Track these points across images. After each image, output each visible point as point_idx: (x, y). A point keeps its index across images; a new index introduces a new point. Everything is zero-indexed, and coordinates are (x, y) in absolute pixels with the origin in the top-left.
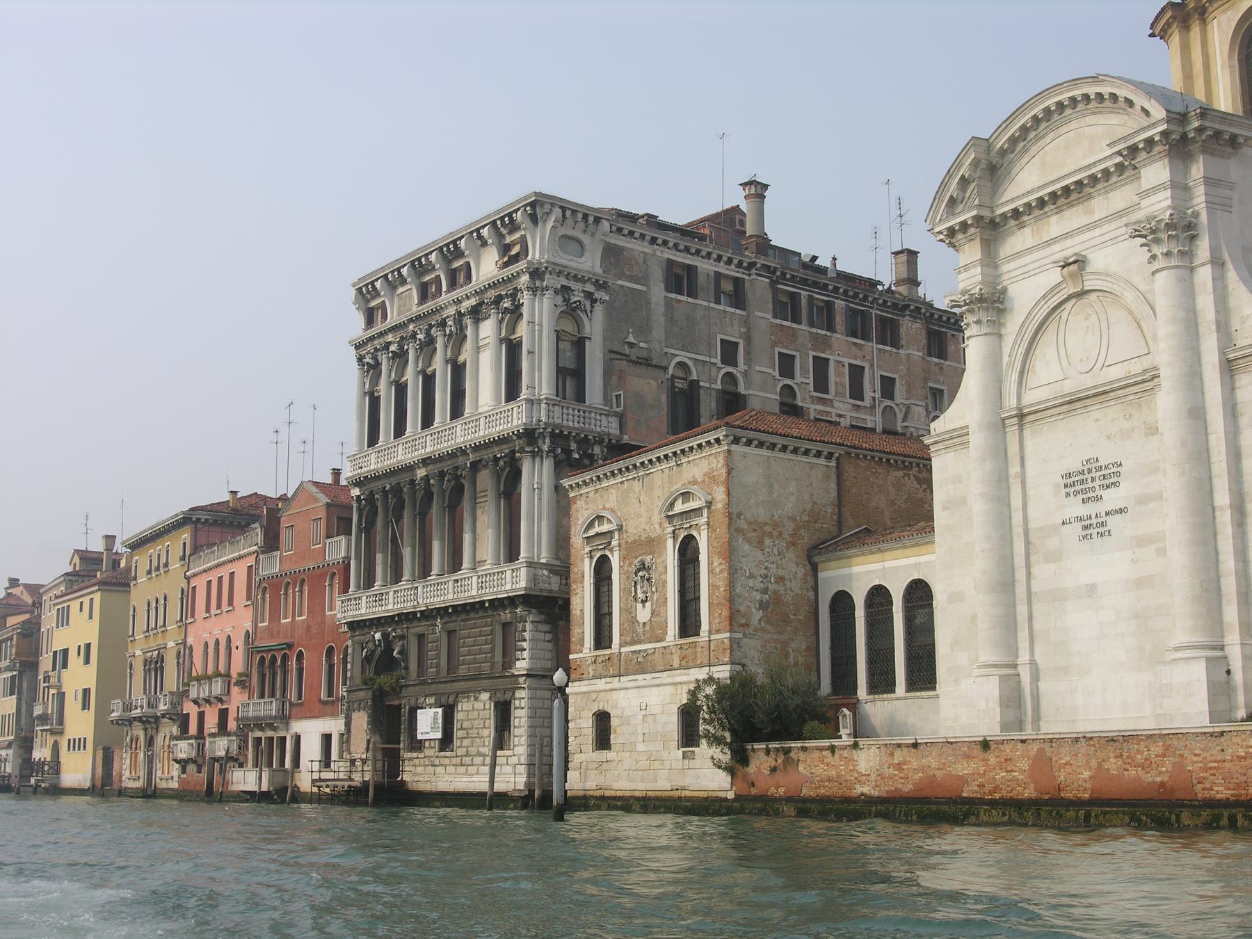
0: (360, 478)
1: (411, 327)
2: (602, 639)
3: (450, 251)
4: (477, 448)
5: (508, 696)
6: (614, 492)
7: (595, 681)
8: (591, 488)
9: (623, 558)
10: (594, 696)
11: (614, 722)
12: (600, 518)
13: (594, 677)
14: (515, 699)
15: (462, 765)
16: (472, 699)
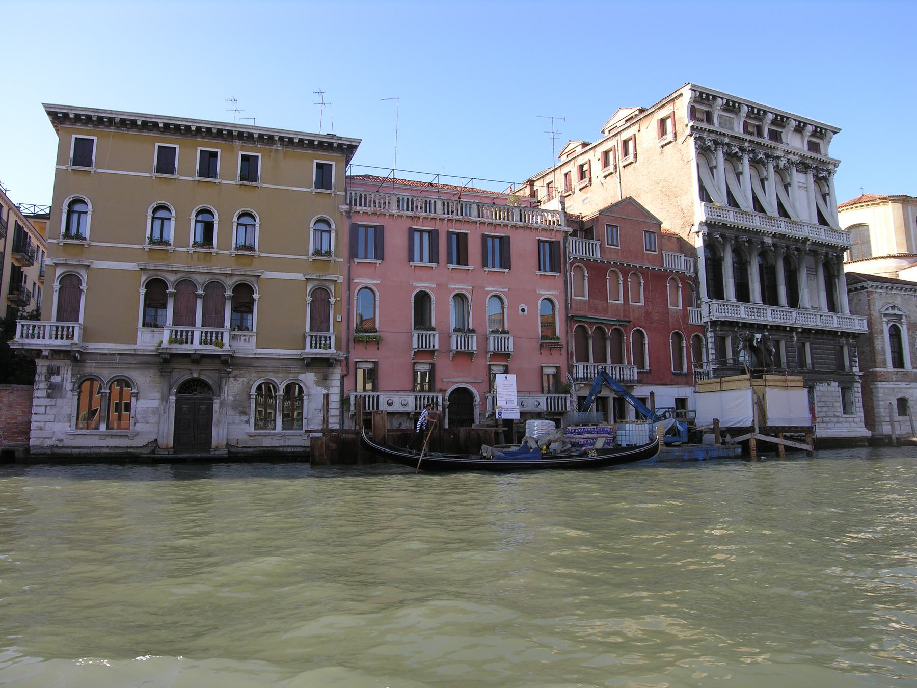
0: (719, 223)
1: (746, 144)
2: (899, 362)
3: (781, 120)
4: (814, 243)
5: (848, 385)
6: (899, 297)
7: (898, 383)
8: (884, 291)
9: (908, 329)
10: (897, 390)
11: (910, 403)
12: (893, 307)
13: (896, 381)
14: (854, 387)
15: (823, 422)
16: (826, 385)
